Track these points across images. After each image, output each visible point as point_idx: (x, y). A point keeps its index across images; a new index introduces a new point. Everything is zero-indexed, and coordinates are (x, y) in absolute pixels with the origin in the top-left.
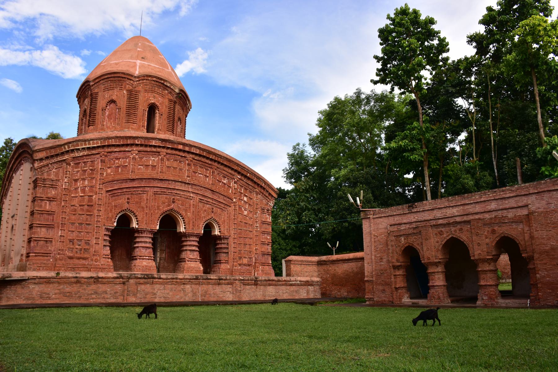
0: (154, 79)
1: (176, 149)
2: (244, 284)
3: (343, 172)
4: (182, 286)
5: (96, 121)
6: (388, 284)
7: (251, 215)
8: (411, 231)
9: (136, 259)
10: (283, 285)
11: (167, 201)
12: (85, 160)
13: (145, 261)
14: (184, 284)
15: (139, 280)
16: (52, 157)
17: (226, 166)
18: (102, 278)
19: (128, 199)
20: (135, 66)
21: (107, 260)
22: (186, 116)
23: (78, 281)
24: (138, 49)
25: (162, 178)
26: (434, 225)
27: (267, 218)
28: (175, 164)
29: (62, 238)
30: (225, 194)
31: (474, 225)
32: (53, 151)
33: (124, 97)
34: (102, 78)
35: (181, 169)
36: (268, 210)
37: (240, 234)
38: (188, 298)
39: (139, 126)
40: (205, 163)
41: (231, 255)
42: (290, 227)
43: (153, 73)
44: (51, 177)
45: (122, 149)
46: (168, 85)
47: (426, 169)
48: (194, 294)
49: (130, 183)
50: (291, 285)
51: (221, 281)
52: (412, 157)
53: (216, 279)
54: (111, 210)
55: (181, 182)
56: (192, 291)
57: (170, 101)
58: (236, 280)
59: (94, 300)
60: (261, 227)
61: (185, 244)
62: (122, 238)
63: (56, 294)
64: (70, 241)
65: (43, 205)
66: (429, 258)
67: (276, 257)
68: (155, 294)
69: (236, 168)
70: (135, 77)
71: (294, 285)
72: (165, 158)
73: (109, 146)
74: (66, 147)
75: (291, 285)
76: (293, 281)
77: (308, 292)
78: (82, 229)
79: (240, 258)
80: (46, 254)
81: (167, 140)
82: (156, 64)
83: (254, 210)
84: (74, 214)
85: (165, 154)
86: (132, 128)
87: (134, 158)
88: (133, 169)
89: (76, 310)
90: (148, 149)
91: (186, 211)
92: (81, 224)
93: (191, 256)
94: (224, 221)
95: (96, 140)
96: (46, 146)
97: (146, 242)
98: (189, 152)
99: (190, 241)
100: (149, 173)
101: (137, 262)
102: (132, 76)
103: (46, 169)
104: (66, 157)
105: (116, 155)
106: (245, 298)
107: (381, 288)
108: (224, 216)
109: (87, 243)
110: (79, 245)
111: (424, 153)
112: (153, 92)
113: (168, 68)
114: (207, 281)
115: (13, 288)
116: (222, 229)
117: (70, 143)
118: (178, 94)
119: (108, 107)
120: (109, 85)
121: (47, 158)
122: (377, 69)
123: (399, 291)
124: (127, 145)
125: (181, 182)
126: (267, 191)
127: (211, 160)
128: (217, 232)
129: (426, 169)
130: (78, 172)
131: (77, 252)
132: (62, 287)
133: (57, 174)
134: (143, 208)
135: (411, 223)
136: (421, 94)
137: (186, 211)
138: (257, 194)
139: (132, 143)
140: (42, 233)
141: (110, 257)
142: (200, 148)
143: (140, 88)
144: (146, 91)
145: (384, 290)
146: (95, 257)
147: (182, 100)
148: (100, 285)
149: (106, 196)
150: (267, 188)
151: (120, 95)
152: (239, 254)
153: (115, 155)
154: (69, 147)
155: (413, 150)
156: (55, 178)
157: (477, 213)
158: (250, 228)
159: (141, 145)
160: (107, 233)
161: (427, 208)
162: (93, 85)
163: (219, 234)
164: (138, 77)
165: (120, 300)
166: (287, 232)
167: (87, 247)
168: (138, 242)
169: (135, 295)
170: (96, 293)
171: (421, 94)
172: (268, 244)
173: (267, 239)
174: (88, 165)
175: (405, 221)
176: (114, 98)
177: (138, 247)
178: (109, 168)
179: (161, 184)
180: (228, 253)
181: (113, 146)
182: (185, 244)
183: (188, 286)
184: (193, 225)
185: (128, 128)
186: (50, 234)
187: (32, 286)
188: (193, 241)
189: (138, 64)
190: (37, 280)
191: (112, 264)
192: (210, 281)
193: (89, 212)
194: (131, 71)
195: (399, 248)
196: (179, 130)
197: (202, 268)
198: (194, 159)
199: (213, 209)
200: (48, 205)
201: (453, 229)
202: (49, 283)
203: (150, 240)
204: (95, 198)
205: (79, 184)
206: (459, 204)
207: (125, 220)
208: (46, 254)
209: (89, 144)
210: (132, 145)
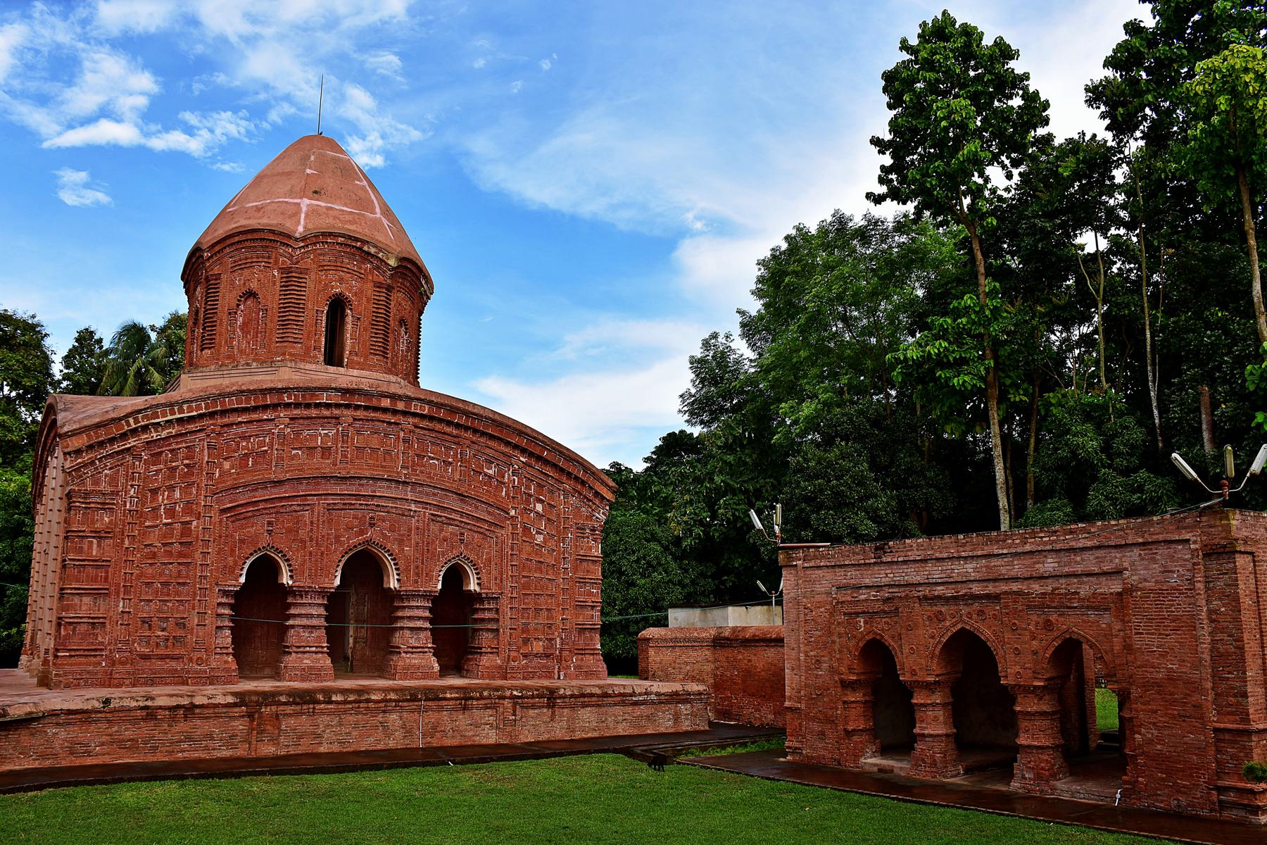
0: (340, 240)
1: (376, 409)
2: (522, 707)
3: (807, 409)
4: (380, 717)
5: (217, 337)
6: (830, 721)
7: (551, 544)
8: (878, 606)
9: (290, 653)
10: (615, 705)
11: (356, 522)
12: (174, 446)
13: (307, 659)
14: (384, 712)
15: (281, 708)
16: (101, 444)
17: (492, 437)
18: (202, 706)
19: (270, 523)
20: (298, 213)
21: (226, 658)
22: (421, 313)
23: (150, 714)
24: (309, 171)
25: (344, 474)
26: (925, 598)
29: (126, 616)
30: (491, 501)
31: (1007, 607)
32: (102, 431)
33: (274, 284)
34: (228, 242)
35: (388, 453)
36: (593, 530)
38: (395, 742)
39: (308, 349)
41: (505, 636)
42: (691, 532)
43: (338, 227)
44: (102, 488)
45: (255, 416)
46: (373, 250)
47: (993, 405)
48: (408, 732)
50: (636, 703)
52: (955, 380)
53: (456, 699)
54: (232, 551)
55: (387, 480)
56: (404, 727)
57: (378, 285)
58: (504, 698)
59: (186, 754)
60: (575, 569)
61: (400, 614)
62: (260, 606)
63: (102, 744)
64: (144, 622)
65: (86, 547)
66: (913, 673)
67: (657, 601)
68: (319, 736)
69: (515, 440)
70: (296, 240)
71: (644, 703)
73: (224, 413)
74: (131, 420)
75: (636, 703)
76: (640, 694)
78: (168, 595)
79: (526, 641)
80: (95, 651)
81: (354, 390)
82: (345, 205)
83: (559, 532)
84: (151, 564)
85: (351, 420)
86: (290, 354)
87: (282, 436)
88: (281, 458)
89: (128, 795)
91: (401, 543)
93: (413, 642)
94: (489, 560)
96: (86, 423)
97: (311, 616)
98: (405, 413)
99: (410, 607)
101: (291, 660)
102: (289, 237)
103: (89, 471)
104: (132, 442)
105: (243, 429)
106: (527, 736)
107: (816, 727)
109: (181, 624)
111: (987, 370)
113: (373, 212)
114: (437, 703)
115: (13, 736)
116: (485, 579)
117: (139, 411)
118: (393, 268)
119: (242, 307)
120: (243, 257)
122: (883, 168)
123: (855, 738)
124: (265, 408)
125: (387, 480)
127: (458, 426)
128: (473, 586)
129: (993, 405)
131: (158, 645)
132: (116, 728)
133: (113, 480)
135: (879, 588)
136: (982, 227)
137: (401, 543)
139: (276, 401)
140: (85, 607)
141: (231, 650)
142: (430, 403)
143: (308, 262)
144: (322, 268)
145: (822, 733)
146: (197, 655)
147: (412, 280)
148: (199, 722)
149: (221, 522)
150: (591, 481)
151: (264, 278)
152: (523, 632)
153: (240, 430)
154: (136, 421)
155: (963, 361)
156: (109, 489)
157: (1015, 579)
159: (297, 405)
160: (224, 600)
161: (913, 555)
162: (208, 259)
163: (478, 589)
164: (304, 239)
165: (241, 752)
166: (684, 544)
167: (180, 633)
168: (295, 616)
169: (274, 741)
170: (189, 739)
171: (982, 227)
174: (180, 456)
175: (867, 581)
176: (254, 285)
177: (293, 626)
178: (225, 459)
180: (497, 630)
182: (400, 614)
183: (394, 716)
185: (284, 354)
186: (102, 607)
187: (51, 731)
189: (304, 209)
190: (63, 717)
191: (234, 666)
192: (445, 703)
193: (185, 556)
194: (288, 225)
195: (853, 642)
196: (403, 347)
197: (436, 667)
199: (462, 534)
200: (95, 546)
201: (964, 610)
202: (88, 722)
203: (322, 611)
204: (197, 527)
206: (979, 553)
207: (264, 570)
208: (95, 651)
209: (181, 411)
210: (275, 407)
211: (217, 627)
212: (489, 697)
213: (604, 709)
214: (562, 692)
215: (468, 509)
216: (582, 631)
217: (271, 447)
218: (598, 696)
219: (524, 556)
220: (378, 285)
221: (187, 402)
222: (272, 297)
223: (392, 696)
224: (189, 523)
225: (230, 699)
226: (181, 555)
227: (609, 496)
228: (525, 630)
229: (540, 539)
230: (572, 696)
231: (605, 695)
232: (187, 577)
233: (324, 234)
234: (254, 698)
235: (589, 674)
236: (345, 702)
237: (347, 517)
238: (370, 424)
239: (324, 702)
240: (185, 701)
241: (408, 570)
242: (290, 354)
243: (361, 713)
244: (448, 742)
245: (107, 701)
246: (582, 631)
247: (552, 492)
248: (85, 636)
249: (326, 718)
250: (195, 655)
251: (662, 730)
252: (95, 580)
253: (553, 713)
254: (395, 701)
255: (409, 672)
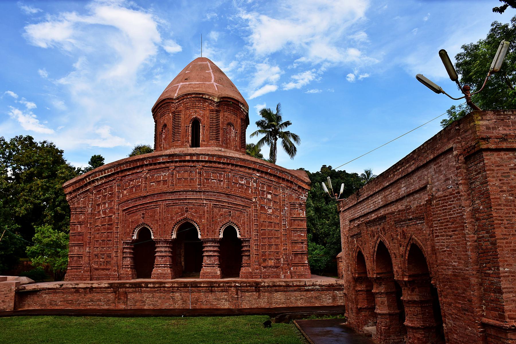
1: (185, 161)
4: (171, 295)
7: (277, 213)
10: (295, 291)
11: (179, 211)
12: (105, 187)
13: (162, 269)
14: (172, 292)
15: (127, 289)
17: (241, 166)
18: (95, 288)
19: (143, 214)
23: (77, 290)
25: (171, 190)
27: (299, 214)
28: (186, 175)
29: (88, 254)
35: (192, 179)
37: (262, 235)
40: (217, 168)
41: (253, 257)
45: (134, 171)
46: (207, 97)
49: (144, 200)
51: (213, 289)
56: (182, 299)
58: (231, 287)
59: (91, 307)
60: (291, 225)
64: (96, 256)
68: (144, 302)
69: (253, 166)
72: (175, 171)
73: (122, 171)
74: (87, 179)
75: (308, 290)
76: (309, 286)
77: (334, 298)
79: (265, 260)
81: (173, 154)
82: (198, 81)
83: (280, 207)
85: (174, 167)
86: (175, 146)
90: (158, 166)
91: (200, 218)
92: (103, 241)
93: (208, 262)
94: (244, 223)
95: (110, 168)
98: (198, 161)
99: (207, 246)
100: (164, 188)
102: (172, 99)
104: (89, 188)
106: (245, 305)
108: (244, 218)
109: (109, 256)
110: (103, 258)
112: (193, 107)
114: (197, 289)
118: (217, 102)
121: (74, 191)
124: (138, 167)
126: (296, 185)
127: (224, 163)
130: (100, 197)
131: (101, 264)
133: (84, 202)
134: (157, 220)
137: (200, 218)
138: (283, 190)
139: (141, 164)
141: (129, 266)
144: (187, 108)
146: (114, 268)
149: (123, 215)
150: (295, 181)
152: (263, 256)
154: (89, 179)
156: (83, 206)
158: (277, 226)
159: (151, 164)
160: (126, 246)
164: (178, 98)
165: (112, 307)
167: (109, 260)
169: (125, 303)
170: (92, 301)
172: (302, 243)
173: (300, 236)
178: (125, 190)
179: (173, 196)
180: (249, 255)
181: (126, 170)
183: (177, 294)
184: (208, 231)
187: (44, 296)
188: (210, 246)
189: (179, 87)
192: (201, 289)
193: (111, 229)
197: (219, 273)
198: (203, 166)
199: (230, 212)
205: (102, 207)
207: (144, 233)
208: (78, 267)
209: (105, 173)
210: (142, 166)
211: (123, 257)
212: (223, 286)
213: (289, 293)
214: (263, 284)
215: (231, 200)
216: (296, 255)
217: (142, 183)
218: (284, 286)
219: (262, 220)
220: (212, 111)
221: (106, 169)
222: (170, 126)
223: (176, 285)
224: (111, 216)
225: (107, 285)
226: (108, 229)
227: (306, 187)
228: (264, 254)
229: (270, 211)
230: (268, 286)
231: (288, 286)
232: (111, 238)
233: (186, 95)
234: (116, 285)
235: (301, 276)
236: (154, 287)
237: (176, 209)
238: (183, 168)
239: (145, 287)
240: (89, 286)
241: (204, 230)
242: (175, 146)
243: (162, 292)
244: (204, 307)
245: (62, 285)
246: (296, 255)
247: (276, 188)
248: (77, 261)
249: (147, 294)
250: (114, 268)
251: (325, 304)
252: (79, 240)
253: (259, 295)
254: (176, 287)
255: (206, 275)
